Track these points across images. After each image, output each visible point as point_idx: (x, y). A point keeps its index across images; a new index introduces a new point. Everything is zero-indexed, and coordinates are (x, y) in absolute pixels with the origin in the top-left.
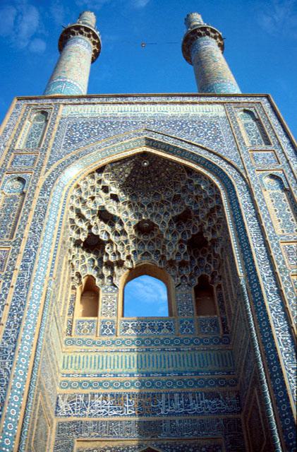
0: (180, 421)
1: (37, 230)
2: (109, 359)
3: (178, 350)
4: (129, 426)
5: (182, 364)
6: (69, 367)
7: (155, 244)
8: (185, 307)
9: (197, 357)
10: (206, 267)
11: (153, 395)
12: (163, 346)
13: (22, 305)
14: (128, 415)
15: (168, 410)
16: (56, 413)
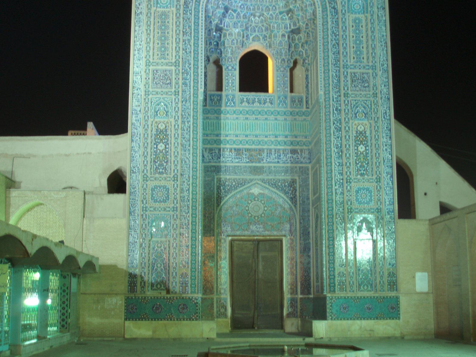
0: (274, 167)
1: (188, 50)
2: (232, 124)
3: (276, 119)
4: (245, 169)
5: (278, 130)
6: (207, 130)
7: (264, 29)
8: (282, 86)
9: (287, 125)
10: (300, 51)
11: (260, 150)
12: (266, 116)
13: (189, 115)
14: (245, 163)
15: (268, 160)
16: (203, 160)
